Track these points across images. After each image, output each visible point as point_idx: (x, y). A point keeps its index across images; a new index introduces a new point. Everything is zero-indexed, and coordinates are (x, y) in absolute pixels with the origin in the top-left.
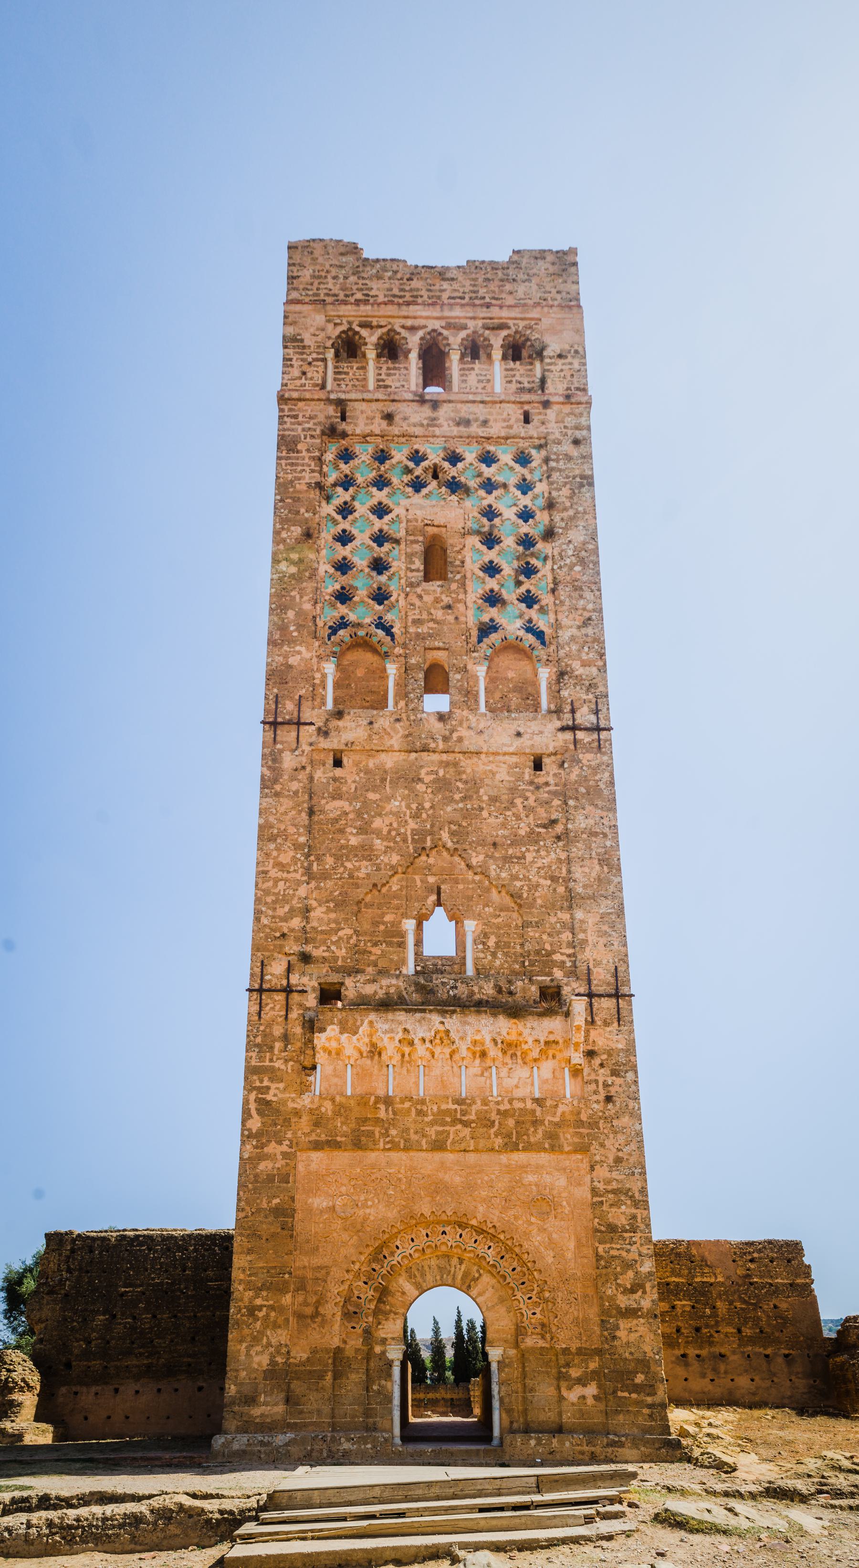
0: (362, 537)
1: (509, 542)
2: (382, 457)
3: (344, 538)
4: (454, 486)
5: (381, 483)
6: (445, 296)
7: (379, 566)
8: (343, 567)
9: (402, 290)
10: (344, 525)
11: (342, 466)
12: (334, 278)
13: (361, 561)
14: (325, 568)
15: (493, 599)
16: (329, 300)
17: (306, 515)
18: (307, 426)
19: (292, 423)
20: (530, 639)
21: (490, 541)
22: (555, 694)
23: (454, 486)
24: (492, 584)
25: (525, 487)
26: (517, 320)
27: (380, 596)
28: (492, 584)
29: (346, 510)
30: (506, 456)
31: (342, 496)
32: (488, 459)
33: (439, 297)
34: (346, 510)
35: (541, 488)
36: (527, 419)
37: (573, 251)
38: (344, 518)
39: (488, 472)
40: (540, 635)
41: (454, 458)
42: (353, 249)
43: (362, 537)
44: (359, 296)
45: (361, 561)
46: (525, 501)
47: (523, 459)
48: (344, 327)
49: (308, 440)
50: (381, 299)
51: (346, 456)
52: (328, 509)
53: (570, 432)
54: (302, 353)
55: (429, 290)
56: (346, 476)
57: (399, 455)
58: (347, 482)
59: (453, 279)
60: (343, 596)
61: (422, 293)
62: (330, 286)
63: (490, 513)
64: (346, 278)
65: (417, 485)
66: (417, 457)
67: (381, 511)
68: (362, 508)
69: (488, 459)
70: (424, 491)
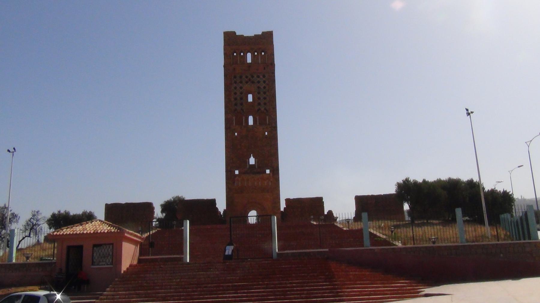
0: (238, 93)
1: (262, 93)
2: (241, 77)
3: (235, 94)
4: (253, 82)
5: (241, 82)
7: (241, 99)
8: (236, 99)
10: (235, 91)
13: (238, 98)
14: (233, 99)
15: (259, 104)
20: (265, 111)
21: (259, 93)
22: (269, 121)
23: (253, 82)
24: (259, 101)
25: (264, 82)
26: (264, 43)
27: (242, 104)
28: (259, 101)
29: (235, 88)
30: (261, 77)
31: (235, 85)
32: (258, 77)
34: (235, 88)
35: (267, 82)
36: (264, 68)
37: (272, 32)
39: (258, 79)
40: (267, 110)
41: (253, 77)
42: (234, 33)
43: (238, 93)
45: (238, 98)
46: (264, 85)
47: (264, 76)
51: (235, 77)
52: (233, 88)
57: (244, 77)
58: (235, 82)
60: (236, 105)
63: (259, 87)
65: (247, 82)
66: (247, 77)
67: (241, 88)
68: (238, 88)
69: (258, 77)
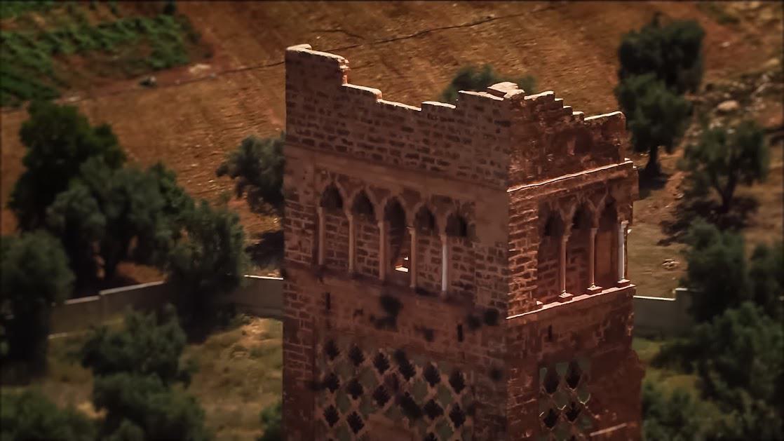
6: (405, 151)
9: (371, 139)
11: (330, 363)
12: (321, 111)
16: (318, 141)
17: (304, 419)
18: (304, 310)
19: (294, 305)
33: (398, 153)
38: (331, 425)
41: (408, 372)
44: (338, 142)
47: (457, 383)
48: (328, 182)
49: (304, 329)
50: (356, 149)
53: (492, 360)
54: (297, 215)
55: (392, 143)
56: (332, 375)
59: (410, 130)
61: (387, 146)
62: (317, 122)
64: (329, 113)
70: (387, 405)
